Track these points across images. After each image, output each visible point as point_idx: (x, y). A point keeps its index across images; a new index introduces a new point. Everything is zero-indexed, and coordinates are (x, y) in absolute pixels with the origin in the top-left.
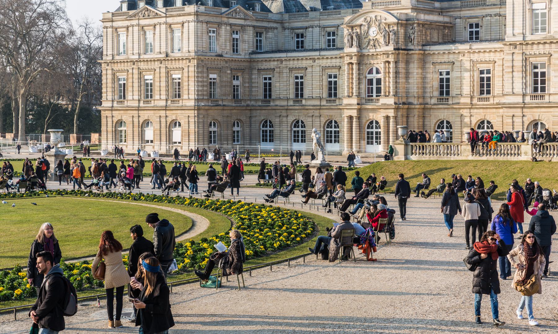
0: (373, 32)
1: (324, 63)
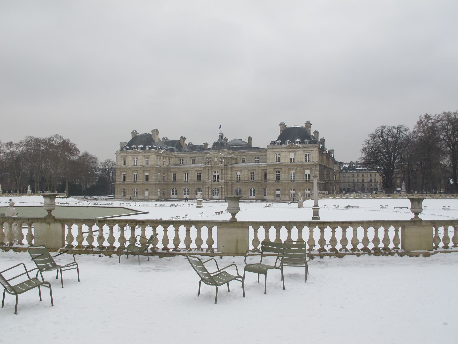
1: (196, 169)
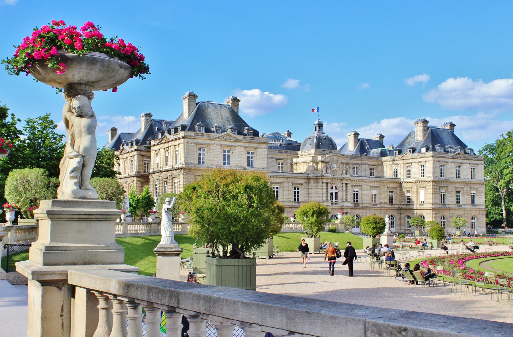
0: (335, 167)
1: (293, 181)
